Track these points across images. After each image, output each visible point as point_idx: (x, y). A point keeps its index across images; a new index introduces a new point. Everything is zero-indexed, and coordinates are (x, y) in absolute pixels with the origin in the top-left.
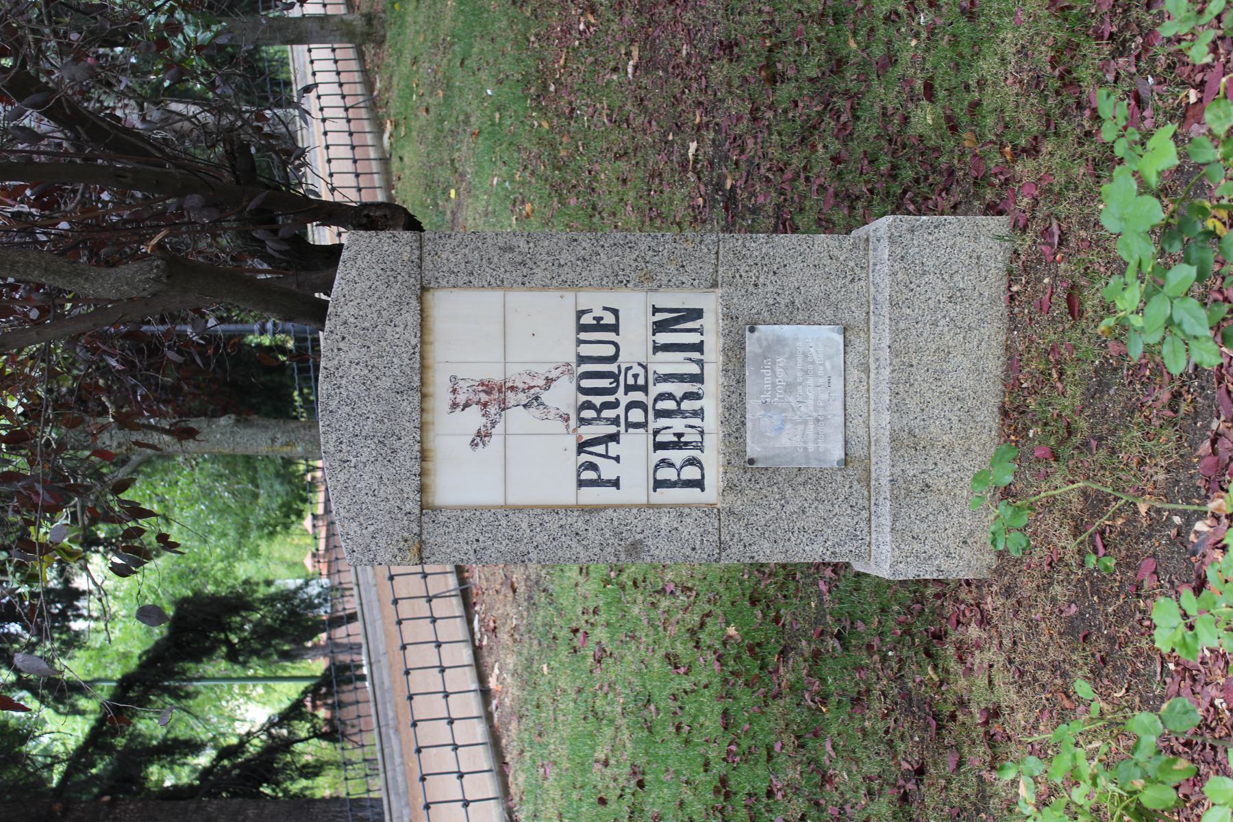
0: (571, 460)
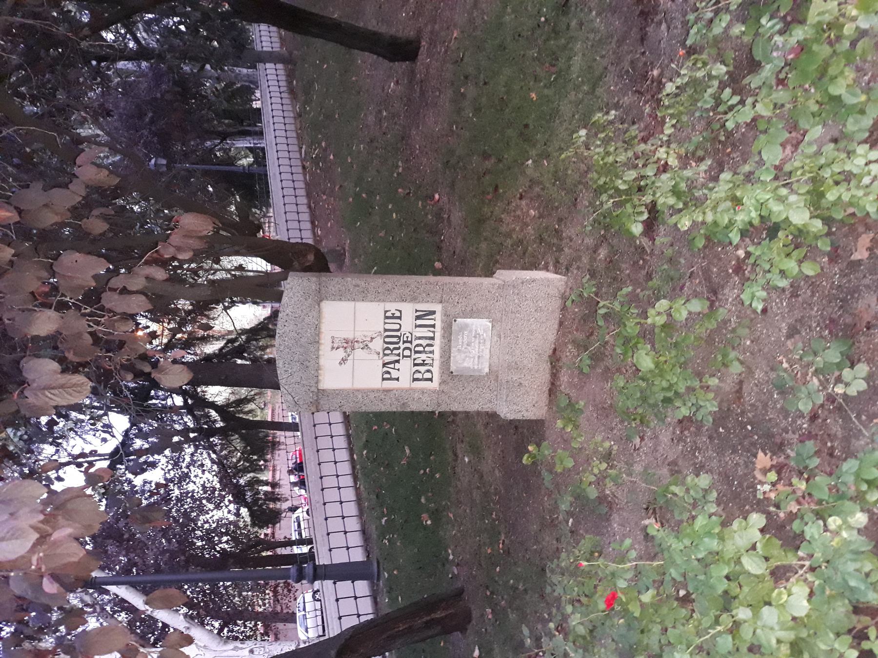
0: (380, 370)
